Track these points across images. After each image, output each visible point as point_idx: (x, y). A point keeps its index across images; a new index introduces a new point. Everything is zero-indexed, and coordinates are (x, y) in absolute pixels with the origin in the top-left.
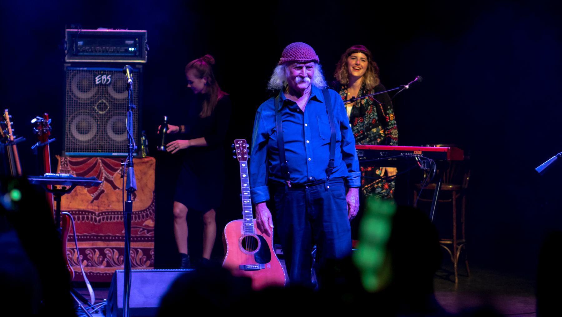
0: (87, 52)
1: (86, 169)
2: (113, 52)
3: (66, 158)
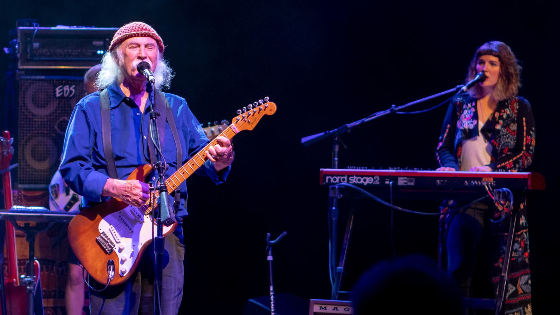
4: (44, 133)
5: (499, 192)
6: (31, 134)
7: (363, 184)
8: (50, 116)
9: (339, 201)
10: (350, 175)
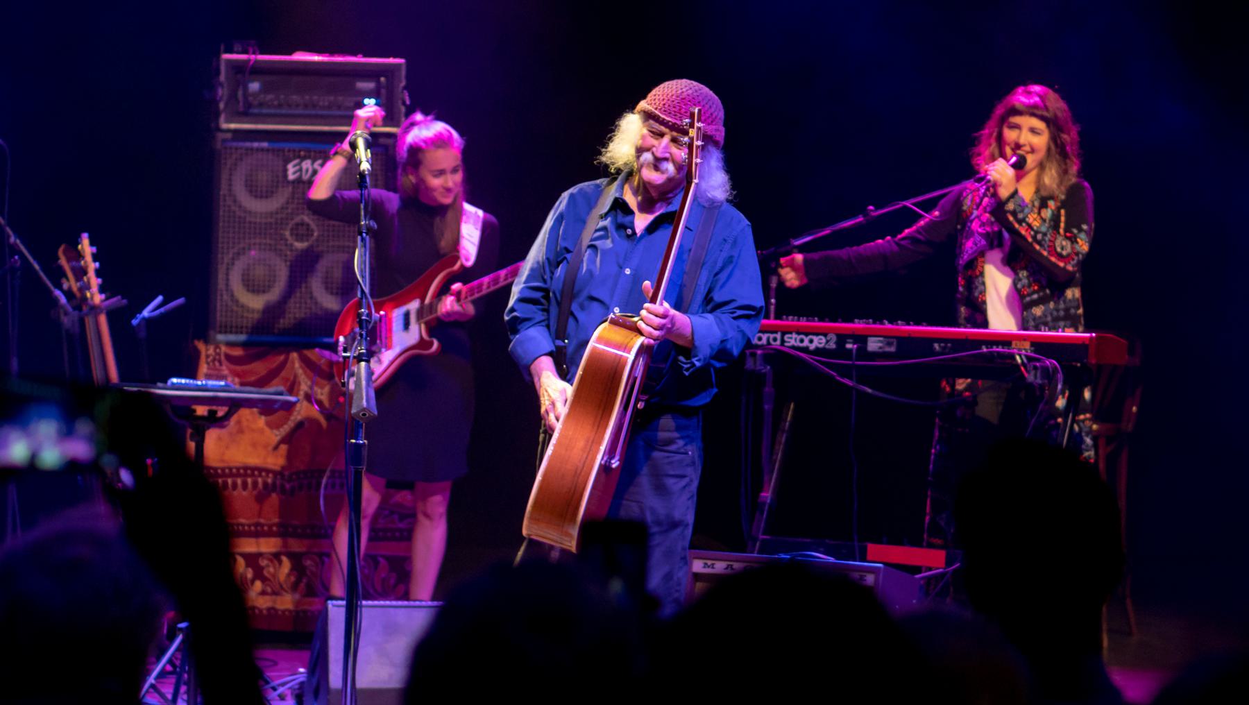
0: (269, 107)
3: (217, 347)
6: (242, 245)
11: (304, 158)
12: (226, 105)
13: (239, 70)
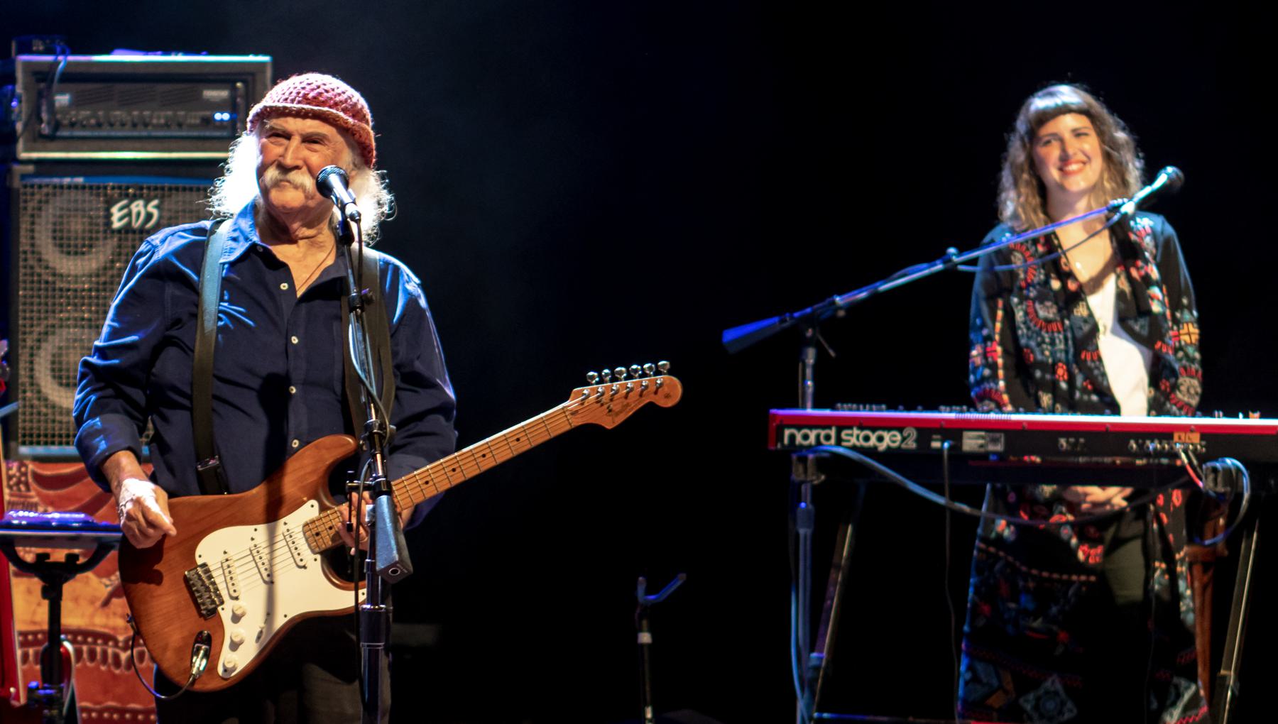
0: (84, 127)
1: (87, 499)
2: (167, 126)
3: (22, 464)
4: (83, 319)
5: (1215, 470)
6: (50, 322)
7: (875, 448)
8: (98, 276)
9: (815, 489)
10: (843, 424)
11: (134, 198)
12: (26, 126)
13: (43, 77)
